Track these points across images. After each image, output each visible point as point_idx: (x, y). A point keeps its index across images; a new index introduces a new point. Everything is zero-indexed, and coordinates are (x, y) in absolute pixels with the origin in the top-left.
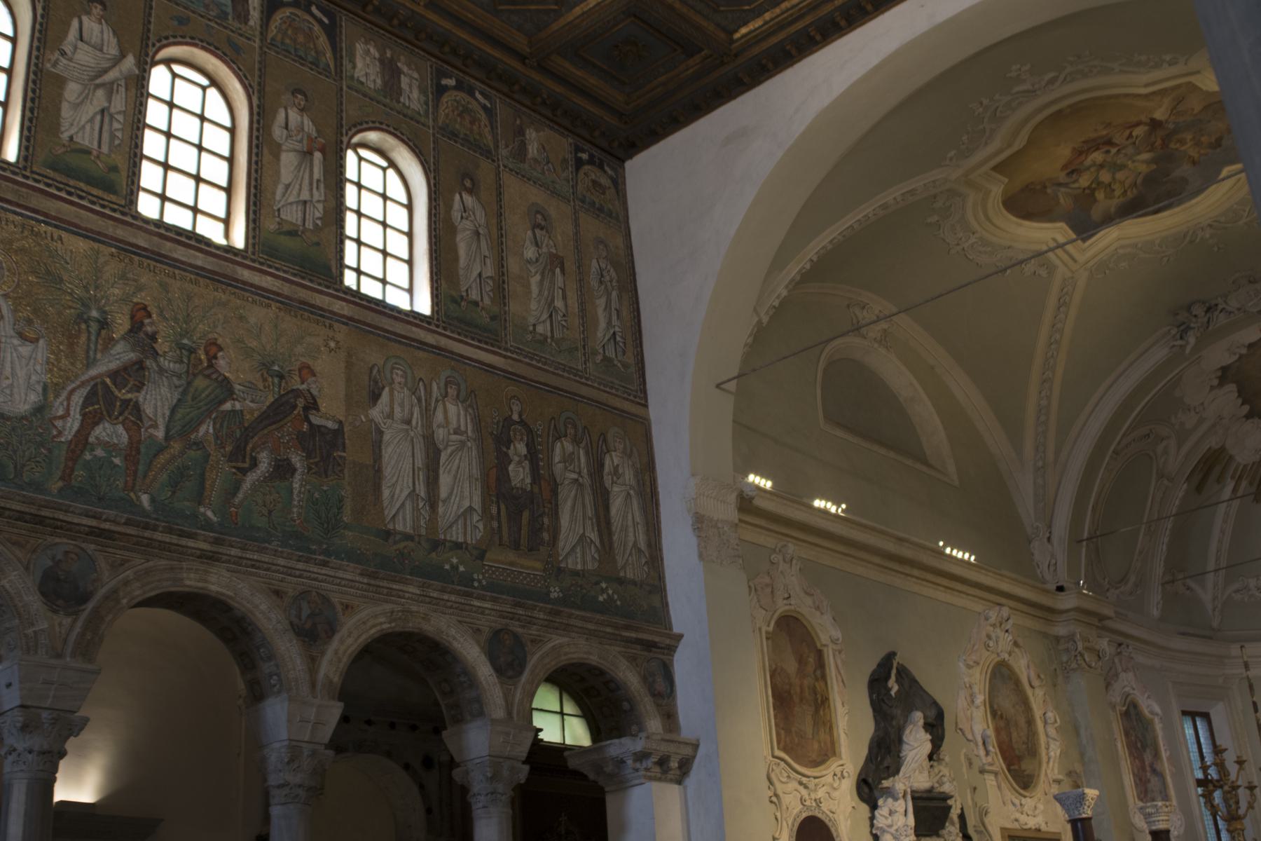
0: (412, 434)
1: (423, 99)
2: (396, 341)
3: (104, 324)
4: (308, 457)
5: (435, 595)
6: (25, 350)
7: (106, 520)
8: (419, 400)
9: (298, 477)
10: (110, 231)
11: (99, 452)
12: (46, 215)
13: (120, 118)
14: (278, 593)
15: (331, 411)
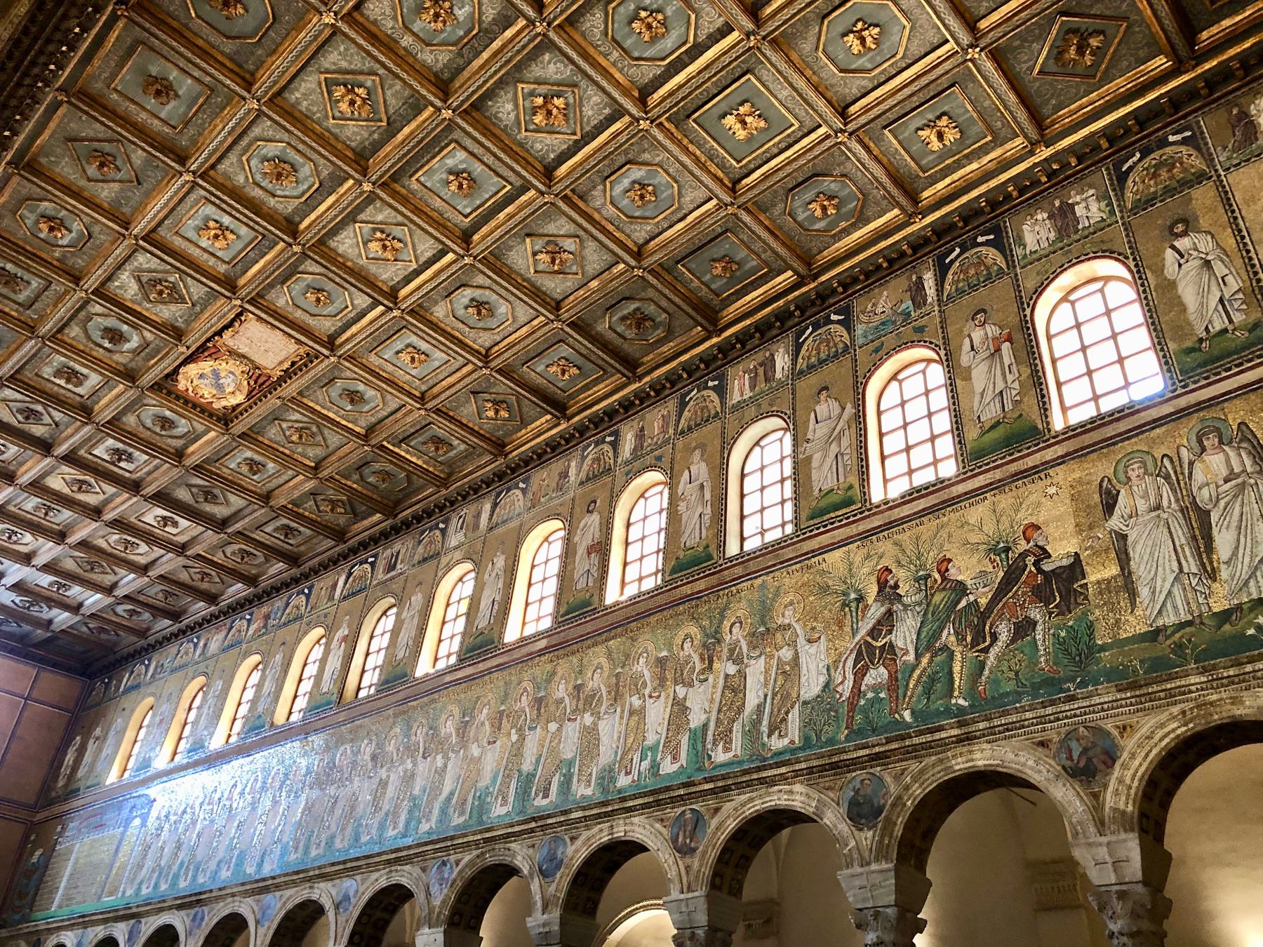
0: (1165, 515)
1: (1103, 204)
2: (1122, 441)
3: (861, 599)
4: (1047, 604)
5: (1231, 673)
6: (813, 649)
7: (874, 746)
8: (1167, 477)
9: (1039, 628)
10: (855, 532)
11: (870, 695)
12: (813, 551)
13: (848, 451)
14: (1042, 744)
15: (1062, 548)
